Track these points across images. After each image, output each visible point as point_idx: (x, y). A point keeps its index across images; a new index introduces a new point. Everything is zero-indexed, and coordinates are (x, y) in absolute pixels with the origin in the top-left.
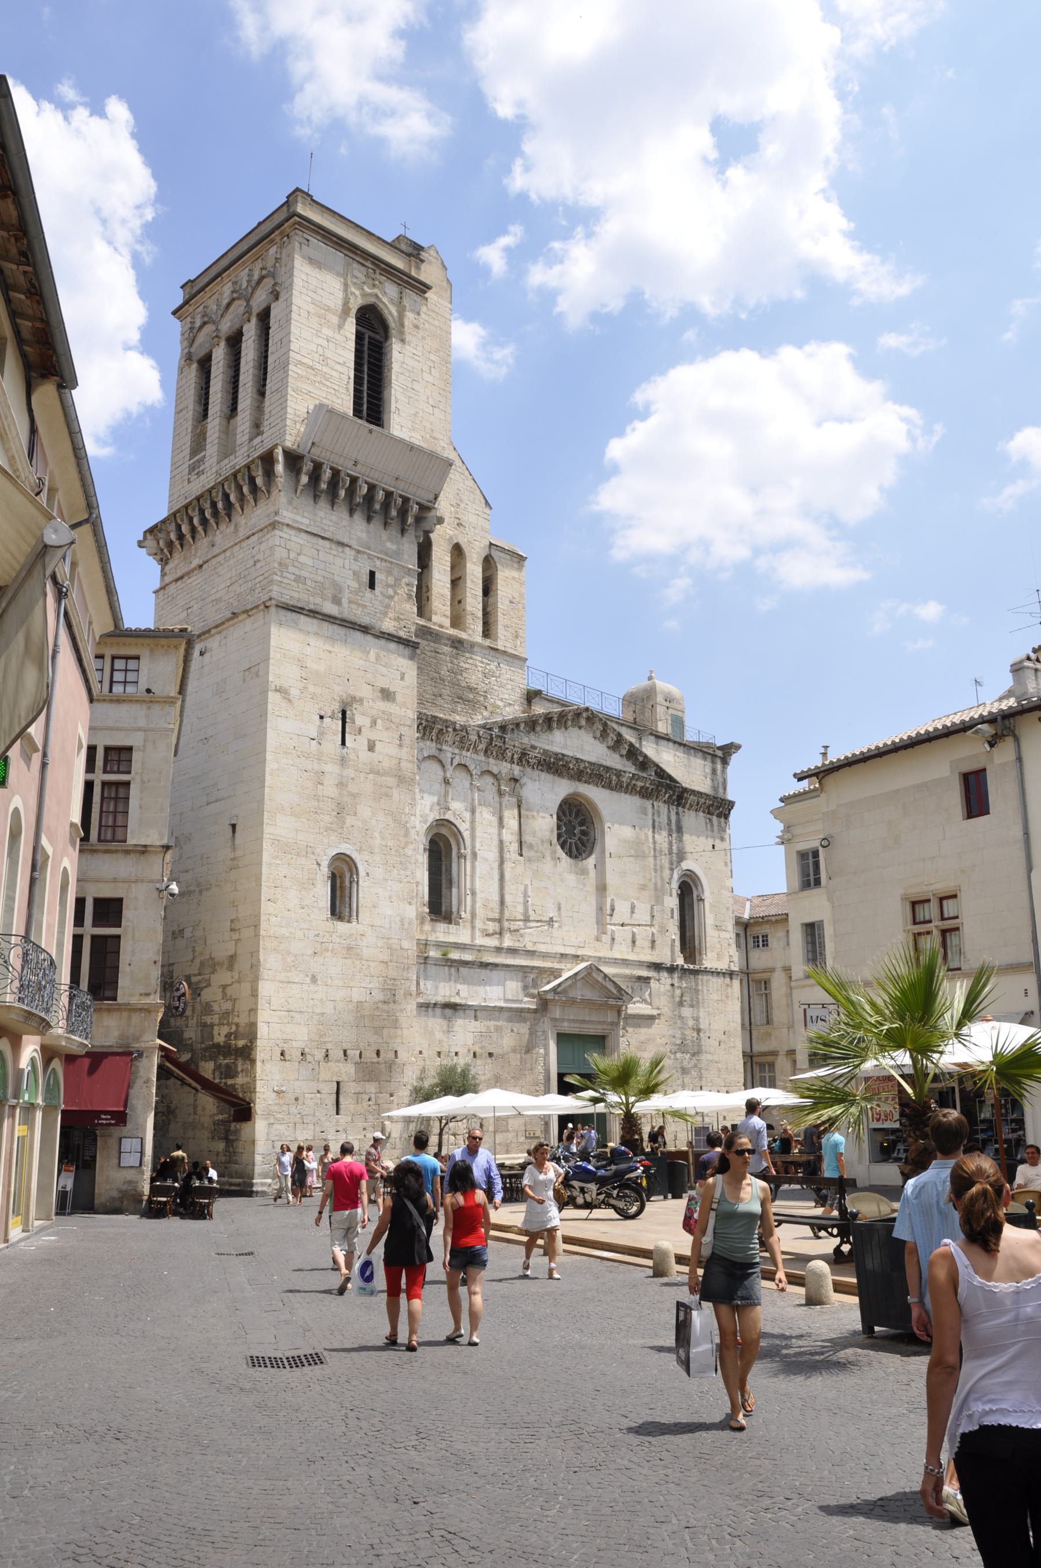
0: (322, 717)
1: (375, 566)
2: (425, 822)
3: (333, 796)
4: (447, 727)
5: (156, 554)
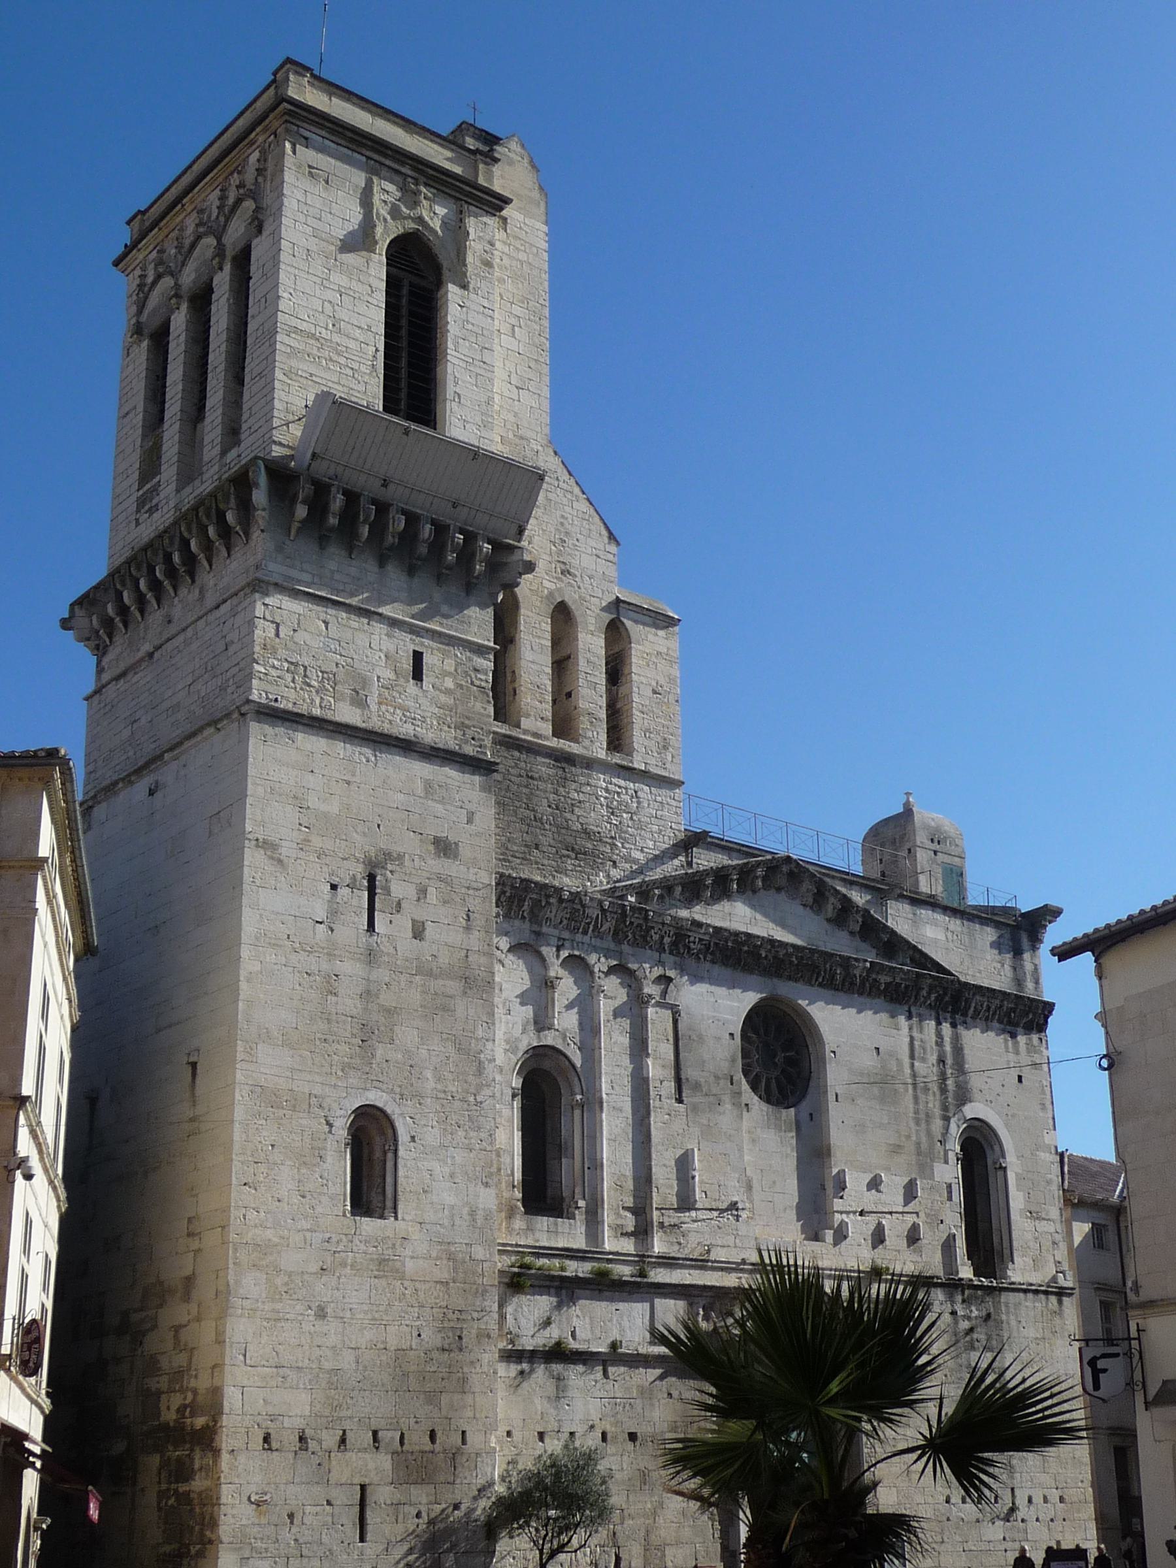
0: (334, 887)
1: (422, 644)
2: (514, 1050)
3: (354, 1012)
4: (548, 896)
5: (88, 639)
